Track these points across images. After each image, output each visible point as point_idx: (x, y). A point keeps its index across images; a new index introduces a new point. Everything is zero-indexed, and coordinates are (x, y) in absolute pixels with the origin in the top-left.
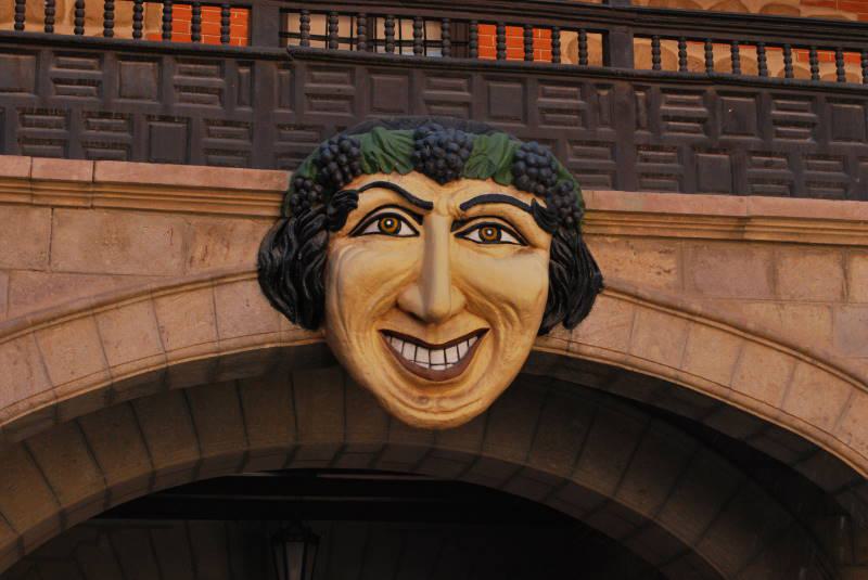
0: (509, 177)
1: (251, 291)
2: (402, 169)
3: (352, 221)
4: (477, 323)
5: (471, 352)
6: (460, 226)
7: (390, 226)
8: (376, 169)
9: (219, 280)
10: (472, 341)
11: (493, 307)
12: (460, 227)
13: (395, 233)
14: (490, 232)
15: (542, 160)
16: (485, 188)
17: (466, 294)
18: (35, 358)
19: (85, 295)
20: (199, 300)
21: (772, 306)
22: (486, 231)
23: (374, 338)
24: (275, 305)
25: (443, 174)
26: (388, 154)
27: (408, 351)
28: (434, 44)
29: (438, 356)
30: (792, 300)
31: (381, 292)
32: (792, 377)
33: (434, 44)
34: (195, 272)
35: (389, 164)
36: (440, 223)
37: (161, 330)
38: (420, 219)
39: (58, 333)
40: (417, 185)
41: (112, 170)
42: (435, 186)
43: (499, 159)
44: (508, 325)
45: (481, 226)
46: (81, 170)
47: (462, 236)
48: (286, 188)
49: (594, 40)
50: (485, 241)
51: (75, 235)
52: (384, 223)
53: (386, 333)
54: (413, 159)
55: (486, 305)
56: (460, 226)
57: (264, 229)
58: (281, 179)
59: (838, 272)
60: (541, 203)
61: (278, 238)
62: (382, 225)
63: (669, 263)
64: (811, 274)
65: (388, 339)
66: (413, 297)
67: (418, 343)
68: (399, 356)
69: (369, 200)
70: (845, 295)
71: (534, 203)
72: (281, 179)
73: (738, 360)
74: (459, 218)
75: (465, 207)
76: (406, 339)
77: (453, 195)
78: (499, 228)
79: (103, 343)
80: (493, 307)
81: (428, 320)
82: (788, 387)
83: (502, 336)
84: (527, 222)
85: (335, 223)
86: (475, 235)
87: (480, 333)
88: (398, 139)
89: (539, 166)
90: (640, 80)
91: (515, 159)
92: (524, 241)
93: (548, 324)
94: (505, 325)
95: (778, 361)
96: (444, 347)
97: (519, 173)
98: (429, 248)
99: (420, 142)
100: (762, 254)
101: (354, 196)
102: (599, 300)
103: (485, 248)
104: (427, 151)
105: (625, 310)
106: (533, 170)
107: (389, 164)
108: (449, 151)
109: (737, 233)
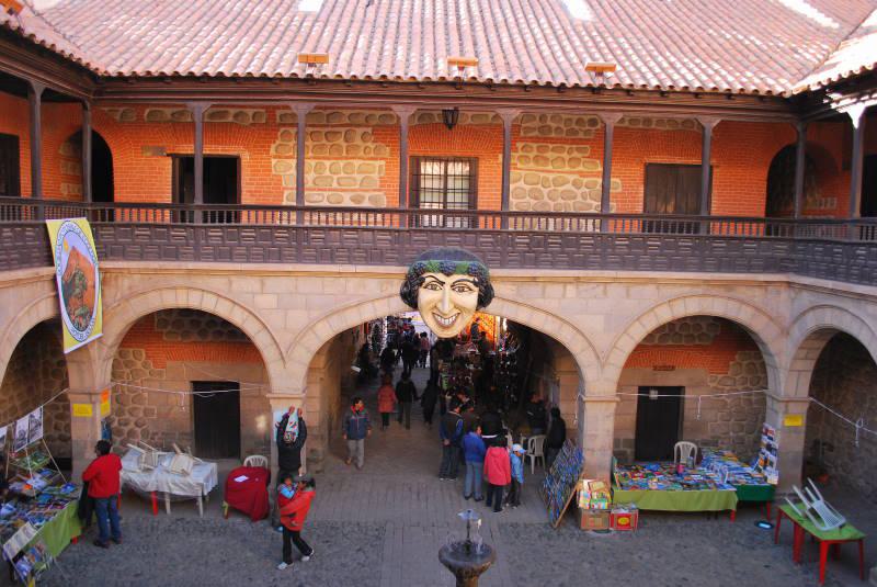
1: (399, 299)
3: (424, 285)
9: (390, 296)
13: (435, 289)
19: (354, 301)
23: (430, 315)
25: (448, 275)
34: (384, 294)
36: (447, 287)
37: (375, 310)
39: (349, 311)
40: (441, 277)
41: (361, 268)
49: (498, 219)
51: (352, 284)
55: (460, 310)
57: (402, 282)
58: (405, 270)
61: (405, 285)
63: (514, 288)
66: (439, 306)
69: (428, 280)
70: (564, 296)
84: (471, 285)
85: (421, 285)
90: (510, 233)
95: (543, 315)
97: (469, 272)
98: (444, 294)
100: (541, 284)
105: (501, 303)
109: (534, 279)
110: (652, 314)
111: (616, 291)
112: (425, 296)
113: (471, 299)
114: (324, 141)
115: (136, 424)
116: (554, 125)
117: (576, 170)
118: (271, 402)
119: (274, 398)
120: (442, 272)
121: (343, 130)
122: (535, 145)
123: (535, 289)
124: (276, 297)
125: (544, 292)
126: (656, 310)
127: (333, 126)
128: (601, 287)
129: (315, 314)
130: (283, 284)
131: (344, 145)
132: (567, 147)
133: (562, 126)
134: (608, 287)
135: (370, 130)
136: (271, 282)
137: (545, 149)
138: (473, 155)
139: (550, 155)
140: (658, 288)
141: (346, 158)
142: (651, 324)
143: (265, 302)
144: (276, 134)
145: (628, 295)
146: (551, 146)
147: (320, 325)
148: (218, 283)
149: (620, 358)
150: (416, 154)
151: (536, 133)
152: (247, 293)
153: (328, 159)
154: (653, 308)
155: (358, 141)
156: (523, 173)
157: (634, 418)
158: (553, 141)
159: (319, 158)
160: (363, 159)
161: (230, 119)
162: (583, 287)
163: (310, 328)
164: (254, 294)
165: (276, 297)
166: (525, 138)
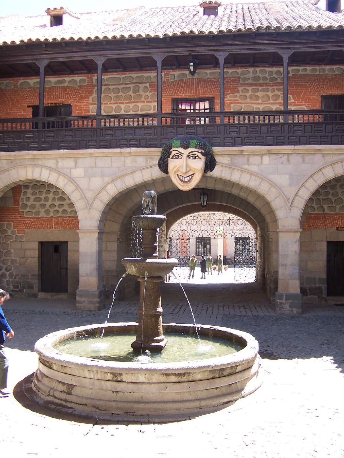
1: (157, 168)
5: (192, 177)
8: (174, 147)
10: (192, 176)
13: (178, 158)
18: (123, 181)
20: (149, 170)
21: (247, 166)
24: (161, 171)
25: (186, 148)
29: (186, 179)
30: (252, 164)
31: (176, 168)
32: (251, 179)
36: (185, 156)
38: (182, 156)
40: (181, 150)
41: (133, 150)
42: (184, 150)
45: (192, 156)
46: (128, 150)
48: (161, 151)
51: (129, 161)
52: (177, 156)
56: (188, 156)
58: (161, 149)
59: (260, 159)
60: (203, 152)
61: (161, 159)
63: (229, 159)
64: (255, 160)
68: (180, 179)
69: (173, 153)
70: (261, 163)
72: (161, 149)
73: (241, 176)
76: (181, 176)
78: (195, 156)
79: (133, 178)
82: (250, 180)
84: (200, 155)
85: (169, 157)
86: (191, 158)
87: (194, 174)
88: (178, 142)
92: (200, 158)
93: (206, 172)
96: (187, 177)
98: (183, 162)
100: (247, 156)
101: (171, 152)
102: (216, 166)
109: (241, 153)
110: (321, 173)
111: (295, 159)
112: (173, 164)
113: (199, 164)
115: (6, 270)
116: (261, 76)
117: (278, 101)
118: (80, 235)
119: (82, 232)
120: (181, 146)
121: (132, 86)
122: (250, 88)
123: (241, 160)
124: (83, 169)
125: (248, 160)
126: (323, 170)
127: (125, 84)
128: (285, 157)
129: (106, 179)
130: (88, 162)
131: (133, 95)
132: (270, 88)
133: (267, 76)
134: (290, 157)
135: (148, 85)
136: (80, 161)
137: (257, 90)
138: (211, 96)
139: (260, 94)
140: (323, 157)
141: (134, 102)
142: (320, 180)
143: (78, 173)
144: (92, 91)
145: (303, 161)
146: (260, 88)
147: (109, 187)
148: (51, 163)
149: (300, 203)
150: (176, 97)
151: (250, 81)
152: (67, 168)
153: (123, 103)
154: (320, 170)
155: (141, 92)
156: (243, 106)
157: (325, 263)
158: (261, 85)
159: (117, 103)
160: (144, 102)
161: (66, 84)
162: (273, 157)
163: (104, 188)
164: (70, 168)
165: (83, 169)
166: (243, 84)
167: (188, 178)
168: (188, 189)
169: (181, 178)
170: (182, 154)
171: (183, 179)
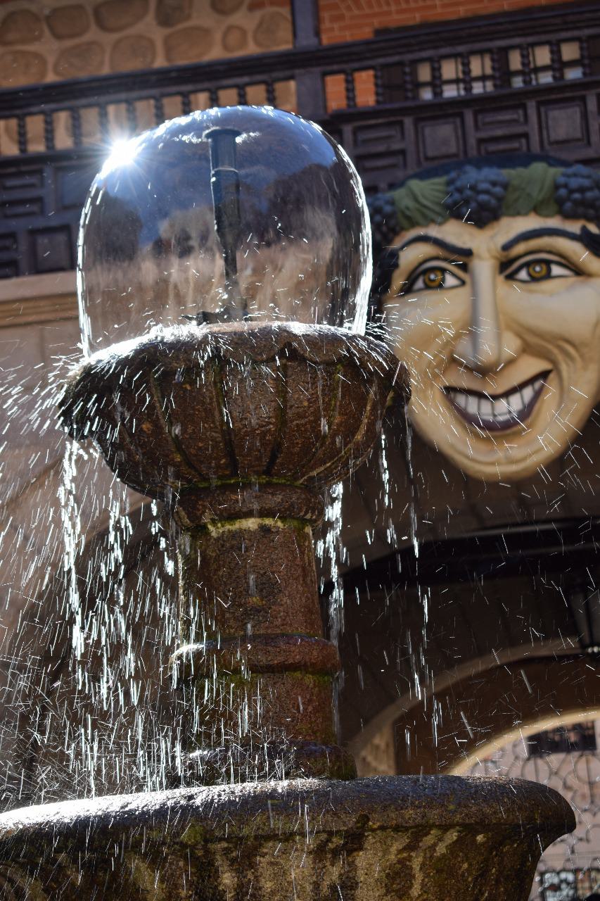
0: (554, 207)
2: (439, 219)
4: (537, 366)
5: (538, 394)
6: (507, 267)
7: (434, 281)
8: (413, 224)
10: (537, 385)
11: (550, 347)
12: (507, 267)
14: (538, 269)
15: (586, 182)
16: (531, 222)
17: (519, 335)
22: (534, 269)
25: (483, 217)
26: (425, 206)
27: (472, 405)
28: (572, 64)
29: (502, 405)
33: (572, 64)
35: (425, 216)
36: (484, 268)
38: (464, 267)
40: (455, 233)
43: (537, 194)
44: (570, 363)
45: (527, 265)
47: (511, 277)
50: (534, 279)
53: (450, 391)
54: (447, 207)
60: (593, 228)
62: (427, 281)
65: (452, 395)
66: (464, 346)
67: (480, 395)
71: (584, 229)
74: (504, 260)
75: (507, 247)
77: (492, 237)
78: (548, 263)
80: (550, 347)
81: (484, 371)
83: (565, 374)
86: (523, 275)
87: (544, 375)
88: (427, 190)
89: (582, 190)
91: (557, 187)
94: (568, 365)
96: (507, 394)
98: (475, 293)
99: (451, 188)
103: (534, 286)
104: (457, 196)
106: (577, 196)
107: (425, 216)
108: (479, 192)
114: (93, 34)
120: (454, 212)
167: (516, 403)
168: (514, 468)
169: (472, 405)
170: (463, 258)
171: (484, 410)
